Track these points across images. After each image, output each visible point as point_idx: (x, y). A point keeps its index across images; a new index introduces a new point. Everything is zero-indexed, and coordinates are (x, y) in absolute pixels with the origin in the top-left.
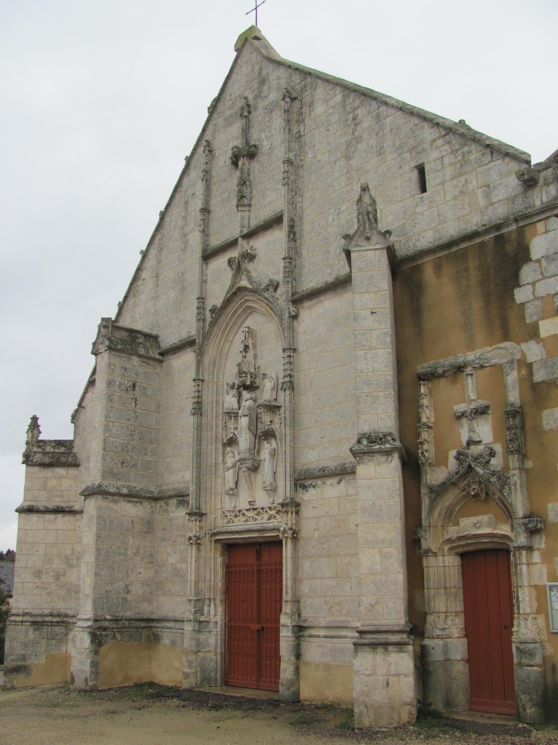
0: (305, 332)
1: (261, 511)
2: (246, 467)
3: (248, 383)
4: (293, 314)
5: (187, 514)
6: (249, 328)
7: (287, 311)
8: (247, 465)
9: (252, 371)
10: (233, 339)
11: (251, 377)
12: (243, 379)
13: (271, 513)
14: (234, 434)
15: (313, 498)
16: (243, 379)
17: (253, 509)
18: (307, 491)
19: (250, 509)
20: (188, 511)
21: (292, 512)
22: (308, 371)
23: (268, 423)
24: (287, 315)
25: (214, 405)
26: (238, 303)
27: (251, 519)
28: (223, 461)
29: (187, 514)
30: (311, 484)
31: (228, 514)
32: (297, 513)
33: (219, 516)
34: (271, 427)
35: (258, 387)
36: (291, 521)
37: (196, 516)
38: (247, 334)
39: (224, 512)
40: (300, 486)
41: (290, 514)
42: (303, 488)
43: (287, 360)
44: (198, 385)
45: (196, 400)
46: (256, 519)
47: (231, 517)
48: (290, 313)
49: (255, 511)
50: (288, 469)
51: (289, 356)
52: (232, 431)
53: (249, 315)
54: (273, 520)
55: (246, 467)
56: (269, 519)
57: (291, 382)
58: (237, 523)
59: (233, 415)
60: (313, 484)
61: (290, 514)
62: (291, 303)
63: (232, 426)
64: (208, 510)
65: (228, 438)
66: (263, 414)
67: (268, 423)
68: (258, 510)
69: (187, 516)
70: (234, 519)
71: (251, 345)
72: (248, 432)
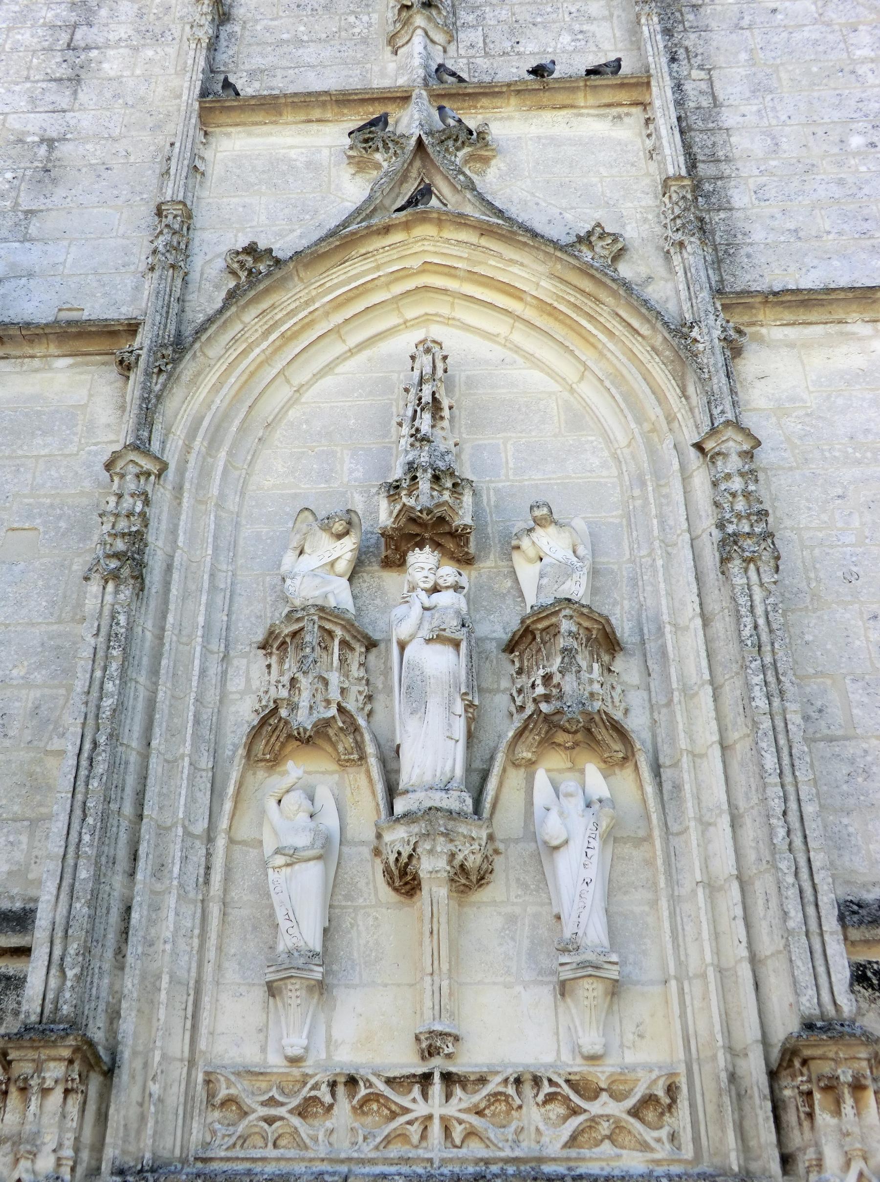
1: (511, 1090)
10: (310, 384)
14: (341, 709)
17: (448, 1078)
19: (426, 1079)
27: (436, 1129)
46: (471, 1133)
47: (282, 1111)
49: (458, 1091)
65: (315, 717)
68: (490, 1088)
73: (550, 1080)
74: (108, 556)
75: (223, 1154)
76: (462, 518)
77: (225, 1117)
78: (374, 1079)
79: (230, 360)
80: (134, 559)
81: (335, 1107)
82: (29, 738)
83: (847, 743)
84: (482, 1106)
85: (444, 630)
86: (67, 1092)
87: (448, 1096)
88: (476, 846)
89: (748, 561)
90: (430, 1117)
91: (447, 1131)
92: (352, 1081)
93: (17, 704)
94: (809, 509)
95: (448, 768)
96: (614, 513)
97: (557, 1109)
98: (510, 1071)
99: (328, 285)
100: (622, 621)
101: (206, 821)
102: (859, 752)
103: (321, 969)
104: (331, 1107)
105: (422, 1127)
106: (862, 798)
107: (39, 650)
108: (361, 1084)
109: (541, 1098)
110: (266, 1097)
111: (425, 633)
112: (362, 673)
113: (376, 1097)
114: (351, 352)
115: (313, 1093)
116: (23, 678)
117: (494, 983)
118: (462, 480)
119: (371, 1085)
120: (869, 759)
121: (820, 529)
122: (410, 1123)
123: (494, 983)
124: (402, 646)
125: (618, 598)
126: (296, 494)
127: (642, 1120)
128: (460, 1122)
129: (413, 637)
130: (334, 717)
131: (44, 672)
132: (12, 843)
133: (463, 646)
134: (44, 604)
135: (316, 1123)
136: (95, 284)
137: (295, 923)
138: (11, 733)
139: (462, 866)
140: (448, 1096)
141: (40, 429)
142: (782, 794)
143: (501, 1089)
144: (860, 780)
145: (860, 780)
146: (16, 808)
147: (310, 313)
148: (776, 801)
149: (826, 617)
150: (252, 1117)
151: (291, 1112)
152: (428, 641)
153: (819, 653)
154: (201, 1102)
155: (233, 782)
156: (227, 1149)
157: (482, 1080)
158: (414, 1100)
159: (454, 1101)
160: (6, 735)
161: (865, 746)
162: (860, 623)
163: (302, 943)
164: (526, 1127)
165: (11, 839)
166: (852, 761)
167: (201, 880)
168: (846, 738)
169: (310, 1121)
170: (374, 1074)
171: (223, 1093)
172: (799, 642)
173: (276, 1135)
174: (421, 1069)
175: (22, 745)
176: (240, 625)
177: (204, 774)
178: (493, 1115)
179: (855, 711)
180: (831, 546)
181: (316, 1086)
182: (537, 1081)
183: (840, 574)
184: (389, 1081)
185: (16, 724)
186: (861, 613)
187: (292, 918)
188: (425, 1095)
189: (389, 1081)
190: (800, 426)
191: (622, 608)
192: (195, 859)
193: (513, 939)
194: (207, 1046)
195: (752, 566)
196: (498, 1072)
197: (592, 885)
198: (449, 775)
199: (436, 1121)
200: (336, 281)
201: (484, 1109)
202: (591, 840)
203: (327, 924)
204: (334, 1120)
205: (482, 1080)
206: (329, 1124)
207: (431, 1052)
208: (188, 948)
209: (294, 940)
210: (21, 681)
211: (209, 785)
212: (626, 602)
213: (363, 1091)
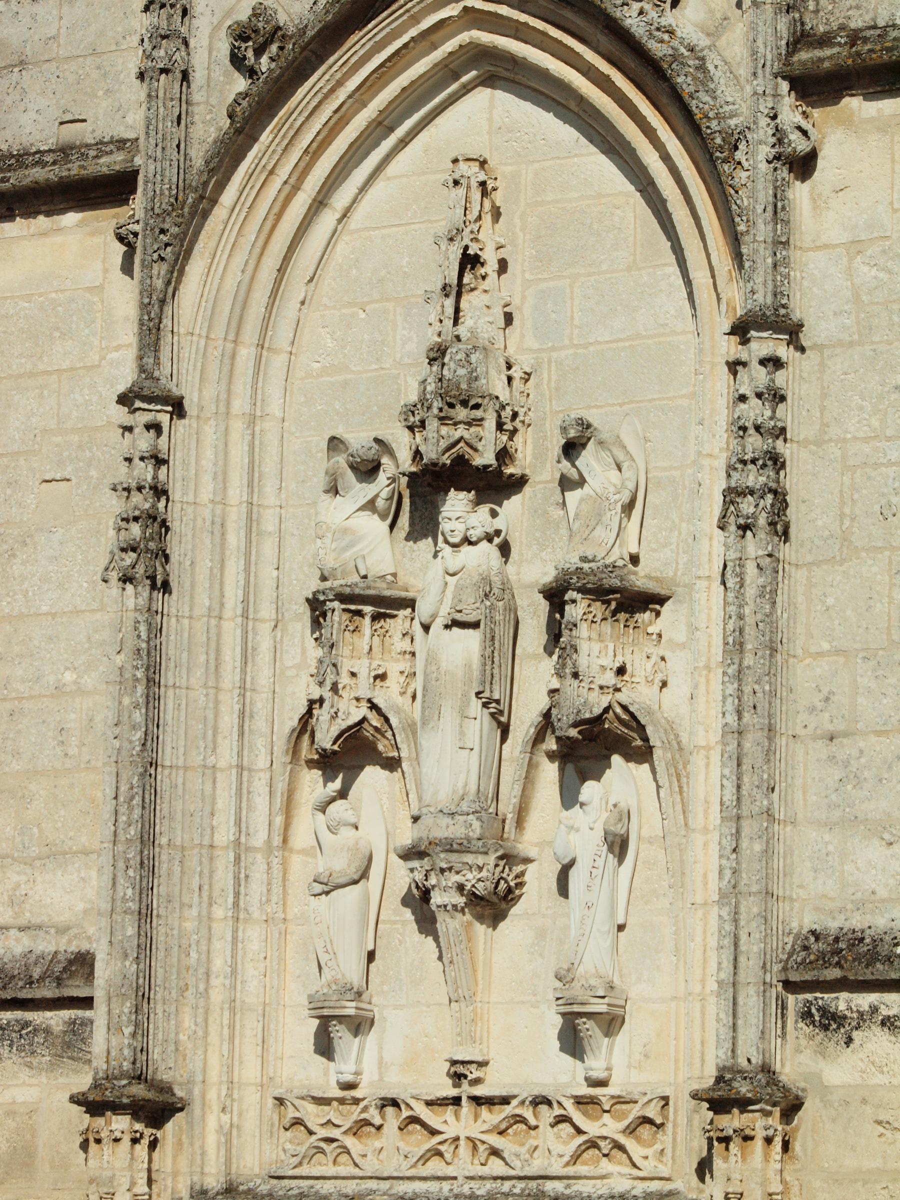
0: (855, 247)
2: (461, 888)
3: (485, 457)
4: (801, 146)
5: (75, 1100)
6: (483, 163)
7: (764, 131)
8: (469, 878)
9: (504, 394)
11: (500, 426)
12: (461, 431)
13: (592, 1128)
14: (373, 707)
15: (879, 1079)
16: (461, 431)
17: (477, 1101)
18: (849, 1041)
19: (457, 1101)
20: (82, 1082)
21: (769, 1140)
22: (867, 449)
23: (610, 679)
24: (765, 151)
25: (235, 540)
26: (415, 19)
27: (464, 1148)
28: (285, 841)
29: (75, 1100)
30: (874, 1010)
31: (313, 1114)
32: (786, 1146)
33: (250, 1123)
34: (622, 697)
35: (518, 483)
36: (765, 1182)
37: (136, 1117)
38: (476, 195)
39: (280, 1101)
40: (806, 1015)
41: (759, 1143)
42: (826, 1028)
43: (761, 375)
44: (155, 427)
45: (142, 502)
46: (495, 1152)
47: (335, 1133)
48: (780, 136)
50: (751, 928)
51: (773, 363)
52: (364, 693)
53: (466, 90)
54: (605, 1166)
55: (461, 888)
56: (576, 1158)
57: (780, 497)
58: (370, 1166)
59: (368, 609)
60: (884, 1011)
61: (759, 1143)
62: (785, 86)
63: (363, 667)
64: (197, 1091)
66: (584, 628)
67: (610, 679)
68: (508, 1110)
69: (80, 1118)
70: (350, 1142)
71: (490, 258)
72: (475, 705)
73: (559, 1103)
74: (123, 550)
75: (290, 1173)
76: (482, 456)
77: (295, 1137)
78: (413, 1103)
79: (248, 204)
80: (147, 550)
81: (385, 1127)
82: (88, 758)
83: (845, 741)
84: (503, 1126)
85: (460, 611)
86: (135, 1141)
87: (476, 1117)
88: (484, 874)
89: (745, 528)
90: (457, 1139)
91: (475, 1148)
92: (395, 1103)
93: (73, 716)
94: (861, 408)
95: (460, 785)
96: (684, 392)
97: (566, 1128)
98: (524, 1095)
99: (353, 60)
100: (678, 554)
101: (267, 831)
102: (855, 753)
103: (353, 1004)
104: (379, 1128)
105: (453, 1147)
106: (847, 810)
107: (86, 646)
108: (403, 1106)
109: (552, 1120)
110: (325, 1121)
111: (444, 615)
112: (406, 645)
113: (414, 1120)
114: (404, 143)
115: (363, 1116)
116: (75, 682)
117: (523, 1002)
118: (483, 397)
119: (412, 1109)
120: (863, 760)
121: (867, 440)
122: (441, 1143)
123: (523, 1002)
124: (426, 628)
125: (677, 520)
126: (346, 383)
127: (638, 1140)
128: (484, 1142)
129: (434, 616)
130: (364, 719)
131: (93, 674)
132: (83, 879)
133: (482, 625)
134: (85, 585)
135: (369, 1142)
136: (95, 74)
137: (332, 955)
138: (71, 753)
139: (474, 894)
140: (476, 1117)
141: (57, 329)
142: (734, 831)
143: (518, 1111)
144: (849, 787)
145: (849, 787)
146: (84, 839)
147: (336, 111)
148: (729, 838)
149: (852, 572)
150: (314, 1137)
151: (345, 1133)
152: (447, 627)
153: (837, 622)
154: (272, 1125)
155: (279, 794)
156: (295, 1167)
157: (505, 1101)
158: (445, 1122)
159: (480, 1121)
160: (66, 755)
161: (862, 744)
162: (887, 578)
163: (339, 976)
164: (541, 1145)
165: (83, 875)
166: (846, 764)
167: (264, 899)
168: (846, 734)
169: (364, 1140)
170: (413, 1097)
171: (291, 1113)
172: (819, 608)
173: (335, 1154)
174: (453, 1092)
175: (82, 766)
176: (294, 577)
177: (262, 774)
178: (515, 1134)
179: (860, 700)
180: (876, 466)
181: (365, 1109)
182: (549, 1103)
183: (877, 508)
184: (429, 1103)
185: (74, 741)
186: (890, 563)
187: (330, 950)
188: (457, 1116)
189: (429, 1103)
190: (874, 272)
191: (680, 533)
192: (258, 875)
193: (541, 955)
194: (275, 1072)
195: (749, 533)
196: (515, 1097)
197: (593, 909)
198: (461, 792)
199: (462, 1142)
200: (362, 52)
201: (507, 1129)
202: (597, 858)
203: (370, 947)
204: (383, 1140)
205: (505, 1101)
206: (378, 1144)
207: (457, 1078)
208: (256, 973)
209: (333, 973)
210: (74, 688)
211: (268, 789)
212: (684, 525)
213: (406, 1113)
